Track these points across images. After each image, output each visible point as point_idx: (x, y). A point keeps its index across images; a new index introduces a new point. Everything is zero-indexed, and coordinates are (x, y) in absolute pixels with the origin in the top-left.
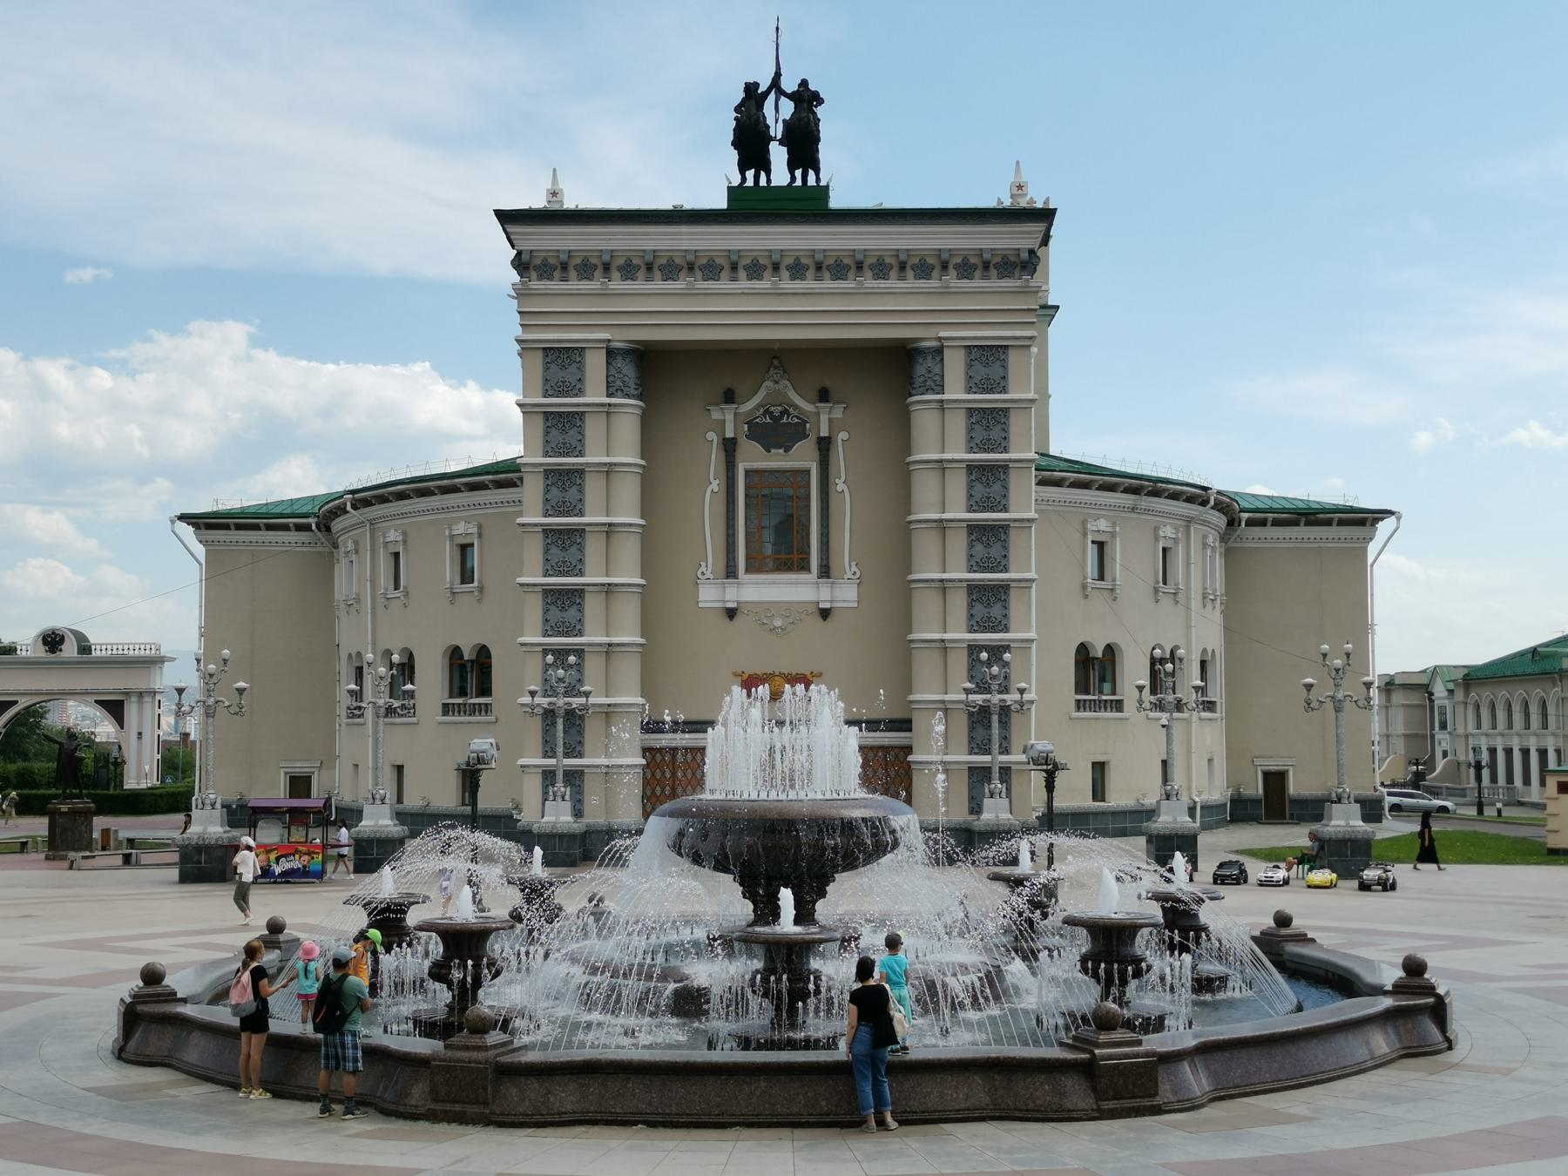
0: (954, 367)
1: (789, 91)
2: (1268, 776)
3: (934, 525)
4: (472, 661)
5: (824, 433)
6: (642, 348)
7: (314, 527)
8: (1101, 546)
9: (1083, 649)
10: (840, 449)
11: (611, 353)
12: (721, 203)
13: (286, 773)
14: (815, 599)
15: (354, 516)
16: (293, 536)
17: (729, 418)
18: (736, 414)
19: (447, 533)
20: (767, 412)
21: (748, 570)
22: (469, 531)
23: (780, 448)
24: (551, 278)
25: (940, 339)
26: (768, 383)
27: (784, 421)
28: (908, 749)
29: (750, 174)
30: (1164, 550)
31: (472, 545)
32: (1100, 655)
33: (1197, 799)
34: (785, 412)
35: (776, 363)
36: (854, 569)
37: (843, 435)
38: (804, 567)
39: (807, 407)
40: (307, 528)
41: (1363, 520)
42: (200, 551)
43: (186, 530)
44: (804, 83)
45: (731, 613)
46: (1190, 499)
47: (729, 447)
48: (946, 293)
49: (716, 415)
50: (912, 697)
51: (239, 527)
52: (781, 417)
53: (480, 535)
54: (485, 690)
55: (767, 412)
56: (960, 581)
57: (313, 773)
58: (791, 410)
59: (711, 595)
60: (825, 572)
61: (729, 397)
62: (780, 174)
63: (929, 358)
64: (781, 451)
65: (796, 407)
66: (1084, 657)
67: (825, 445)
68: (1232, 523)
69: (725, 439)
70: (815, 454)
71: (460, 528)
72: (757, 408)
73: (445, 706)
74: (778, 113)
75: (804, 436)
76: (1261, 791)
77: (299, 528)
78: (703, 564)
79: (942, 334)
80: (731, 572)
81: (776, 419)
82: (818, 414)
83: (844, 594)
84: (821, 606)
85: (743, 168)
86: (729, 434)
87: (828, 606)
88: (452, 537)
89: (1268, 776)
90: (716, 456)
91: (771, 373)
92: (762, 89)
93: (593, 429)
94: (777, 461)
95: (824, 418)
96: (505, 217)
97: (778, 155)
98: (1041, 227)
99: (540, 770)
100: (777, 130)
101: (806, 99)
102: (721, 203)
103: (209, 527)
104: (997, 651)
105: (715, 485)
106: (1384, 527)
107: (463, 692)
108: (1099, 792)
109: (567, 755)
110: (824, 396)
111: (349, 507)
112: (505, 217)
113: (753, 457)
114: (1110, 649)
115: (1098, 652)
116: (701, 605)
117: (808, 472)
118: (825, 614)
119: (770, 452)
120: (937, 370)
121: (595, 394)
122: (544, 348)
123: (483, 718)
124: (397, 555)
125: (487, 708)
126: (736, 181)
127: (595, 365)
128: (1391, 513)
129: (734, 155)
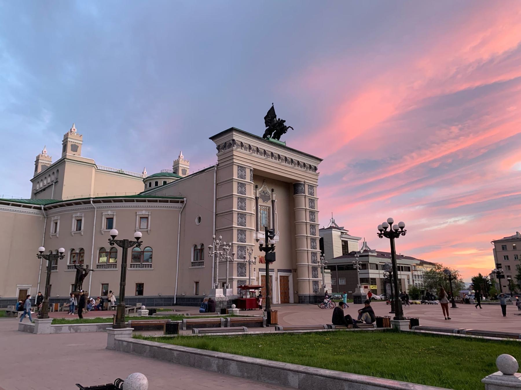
5: (274, 199)
7: (42, 208)
13: (19, 288)
15: (92, 205)
22: (146, 214)
25: (305, 182)
34: (266, 193)
37: (276, 201)
39: (270, 192)
48: (305, 172)
50: (297, 264)
51: (13, 205)
55: (264, 192)
57: (29, 288)
63: (302, 186)
67: (273, 202)
70: (271, 204)
71: (144, 212)
82: (272, 195)
86: (258, 196)
95: (274, 196)
111: (91, 202)
120: (304, 189)
121: (248, 179)
122: (238, 166)
123: (150, 269)
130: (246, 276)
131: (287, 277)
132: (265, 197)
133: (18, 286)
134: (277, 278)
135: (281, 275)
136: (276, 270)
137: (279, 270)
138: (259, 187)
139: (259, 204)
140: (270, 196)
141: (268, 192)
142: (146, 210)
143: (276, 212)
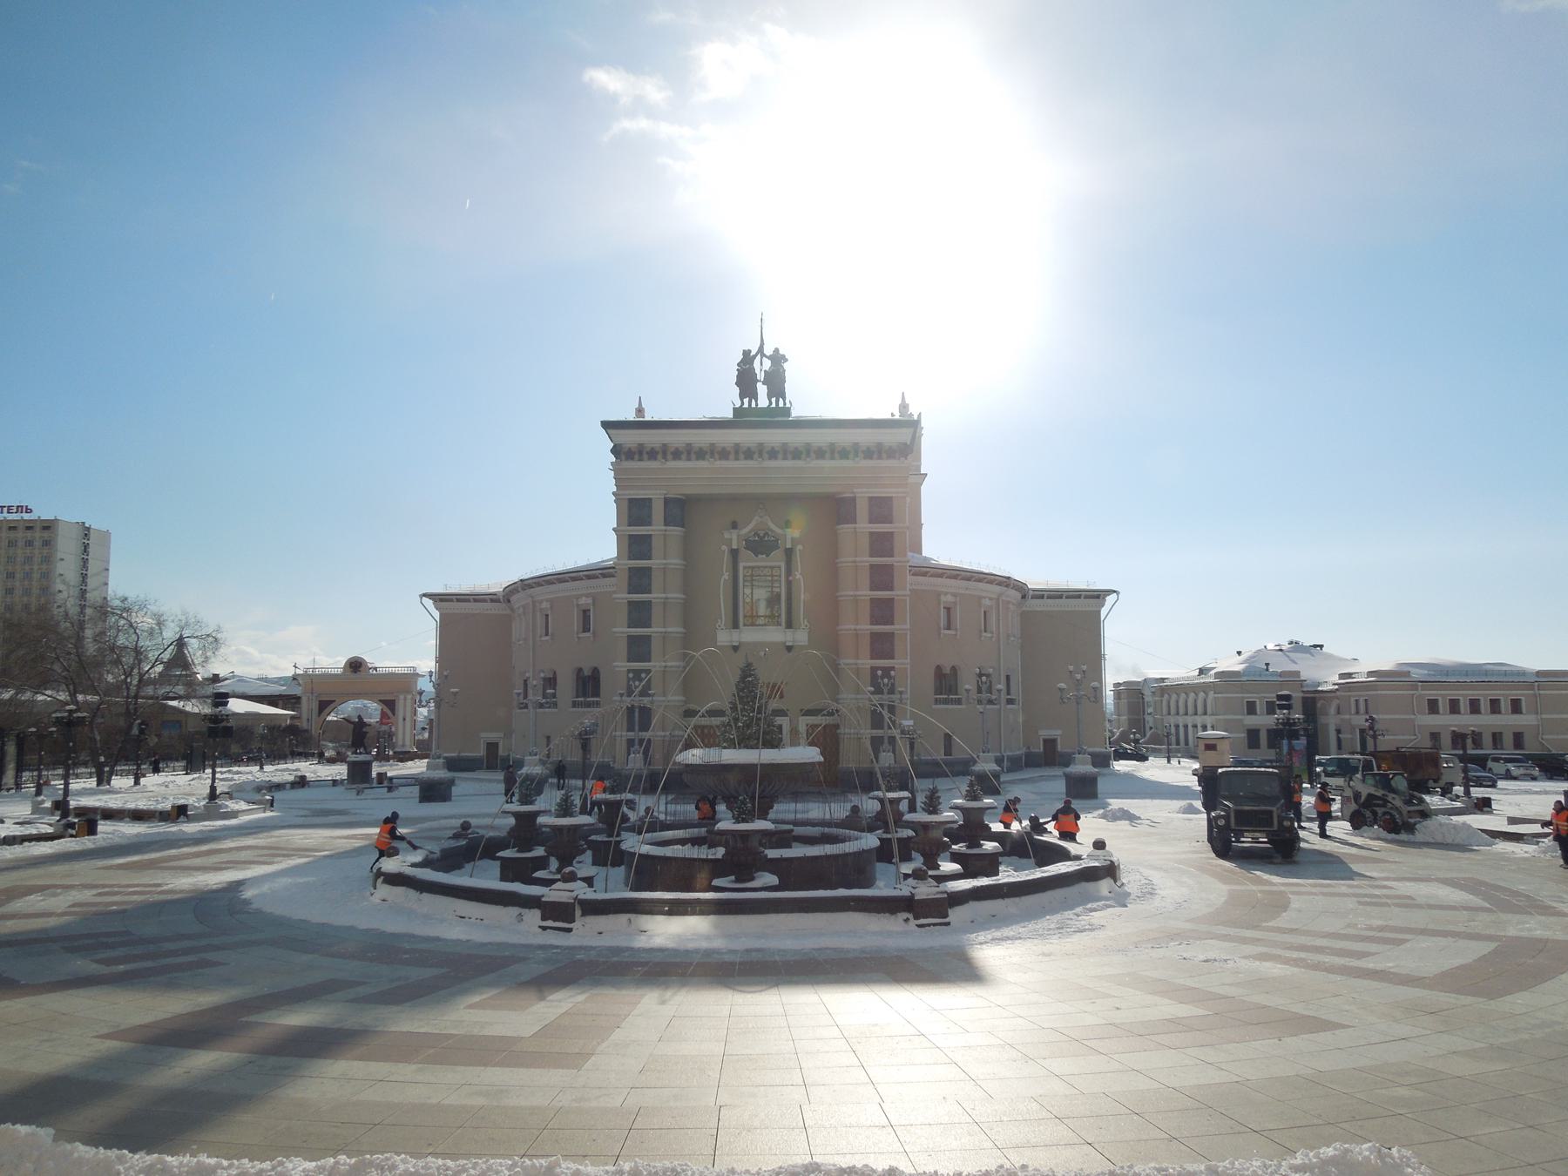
0: (862, 510)
1: (768, 354)
2: (1045, 741)
3: (852, 598)
4: (589, 677)
5: (789, 546)
6: (684, 498)
8: (948, 610)
9: (939, 668)
10: (798, 552)
11: (667, 501)
12: (730, 415)
14: (783, 640)
16: (488, 605)
17: (735, 537)
18: (738, 536)
19: (575, 603)
20: (756, 534)
21: (745, 625)
24: (632, 459)
25: (853, 493)
26: (756, 518)
27: (766, 539)
28: (837, 726)
29: (746, 401)
30: (985, 612)
31: (589, 610)
32: (948, 672)
33: (1005, 754)
34: (765, 535)
35: (761, 506)
36: (806, 623)
37: (800, 547)
38: (779, 624)
40: (497, 601)
41: (1098, 596)
42: (437, 614)
43: (429, 602)
44: (777, 350)
45: (735, 648)
46: (1000, 584)
47: (735, 553)
49: (727, 536)
52: (764, 537)
53: (594, 605)
54: (597, 694)
55: (756, 534)
56: (867, 630)
58: (770, 533)
59: (725, 637)
60: (789, 625)
61: (734, 526)
62: (763, 401)
64: (764, 556)
65: (772, 531)
66: (939, 674)
67: (789, 553)
68: (1024, 597)
69: (732, 549)
72: (750, 532)
73: (574, 702)
74: (761, 367)
76: (1042, 749)
77: (492, 601)
78: (719, 621)
79: (855, 490)
80: (735, 625)
81: (762, 539)
83: (800, 637)
84: (787, 644)
85: (742, 397)
86: (735, 547)
87: (791, 644)
88: (578, 605)
89: (1045, 741)
90: (726, 557)
91: (759, 511)
92: (753, 353)
93: (657, 544)
94: (761, 561)
96: (607, 425)
97: (762, 390)
98: (912, 430)
100: (761, 376)
101: (778, 359)
102: (730, 415)
103: (441, 600)
104: (887, 671)
105: (726, 576)
106: (1110, 599)
107: (585, 695)
108: (948, 752)
109: (641, 730)
112: (607, 425)
113: (747, 561)
114: (954, 669)
115: (947, 671)
116: (718, 644)
117: (779, 567)
118: (789, 649)
119: (757, 556)
124: (547, 615)
125: (597, 704)
126: (738, 404)
127: (658, 511)
128: (1115, 592)
129: (737, 390)
133: (483, 735)
135: (810, 722)
139: (741, 565)
142: (587, 596)
143: (798, 576)
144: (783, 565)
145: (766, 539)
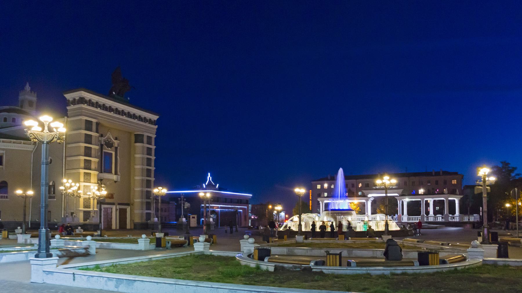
0: (145, 140)
5: (116, 146)
20: (108, 140)
23: (109, 148)
37: (119, 147)
47: (102, 146)
64: (110, 149)
65: (112, 140)
67: (116, 148)
72: (106, 138)
75: (113, 146)
81: (109, 142)
86: (102, 143)
99: (83, 211)
110: (116, 139)
117: (112, 154)
130: (90, 208)
131: (126, 209)
132: (110, 145)
134: (116, 210)
136: (116, 204)
137: (119, 204)
138: (104, 136)
139: (104, 150)
140: (113, 143)
141: (111, 140)
143: (118, 158)
144: (114, 153)
145: (110, 142)
